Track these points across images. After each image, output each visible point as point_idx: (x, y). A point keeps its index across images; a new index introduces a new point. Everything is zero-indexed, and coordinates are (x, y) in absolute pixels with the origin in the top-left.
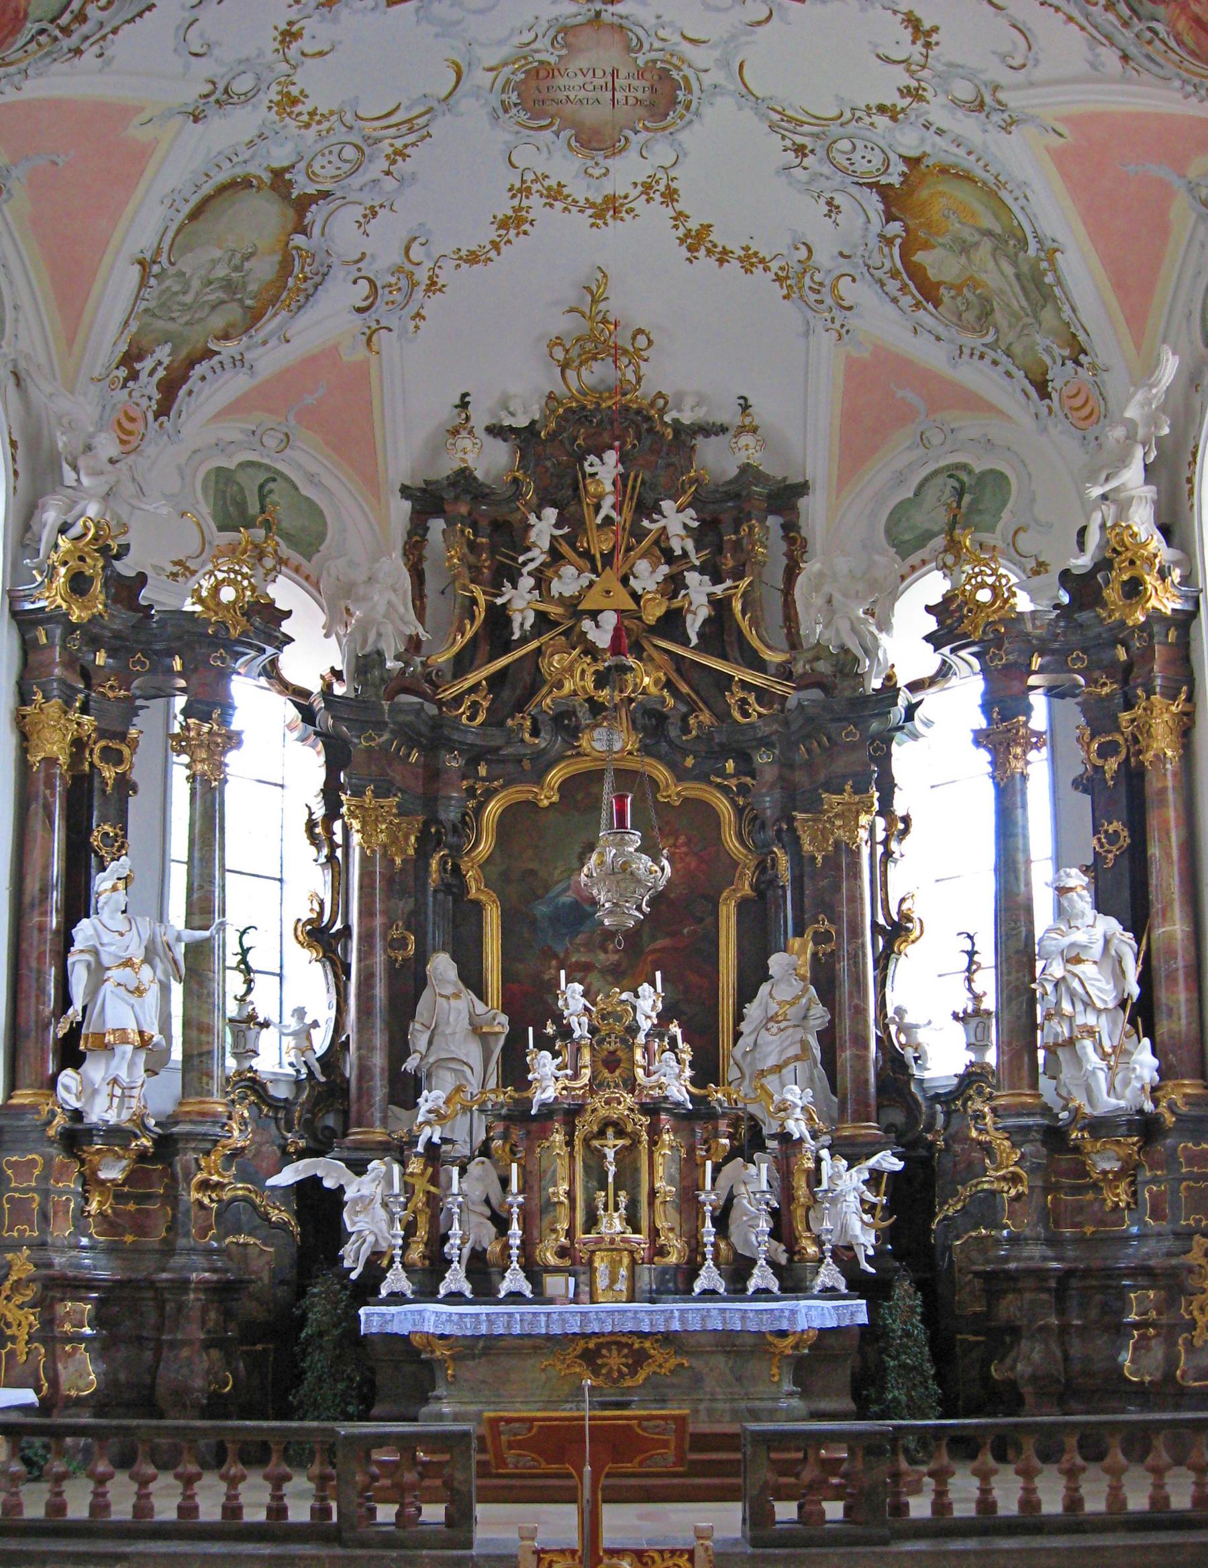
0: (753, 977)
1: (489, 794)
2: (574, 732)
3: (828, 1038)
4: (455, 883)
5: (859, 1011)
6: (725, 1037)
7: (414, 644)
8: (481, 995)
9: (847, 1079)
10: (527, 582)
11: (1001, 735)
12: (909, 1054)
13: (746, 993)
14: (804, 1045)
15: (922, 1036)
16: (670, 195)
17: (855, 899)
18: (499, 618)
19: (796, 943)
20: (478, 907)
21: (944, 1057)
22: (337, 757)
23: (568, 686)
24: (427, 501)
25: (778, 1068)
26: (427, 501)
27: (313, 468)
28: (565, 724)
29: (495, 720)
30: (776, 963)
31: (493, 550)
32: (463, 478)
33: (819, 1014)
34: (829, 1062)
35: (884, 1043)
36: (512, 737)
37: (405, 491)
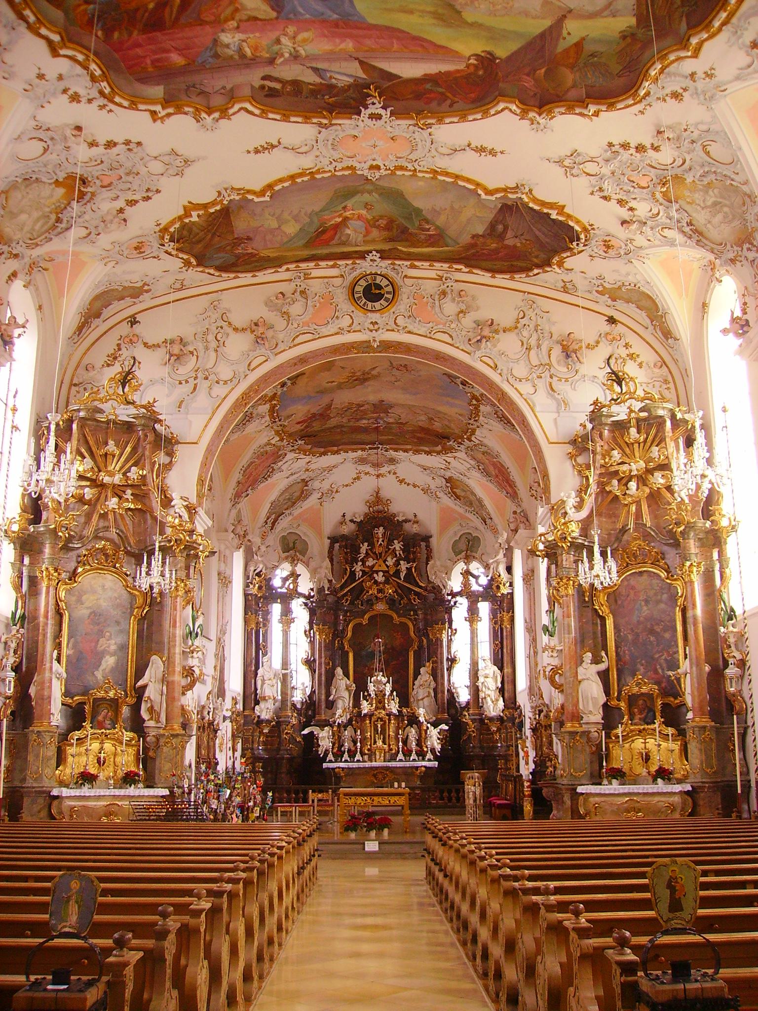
0: (417, 674)
1: (350, 621)
2: (372, 605)
3: (435, 690)
4: (342, 647)
5: (443, 684)
6: (410, 690)
7: (330, 581)
8: (348, 676)
9: (440, 701)
10: (360, 563)
11: (473, 615)
12: (455, 695)
13: (415, 678)
14: (429, 693)
15: (459, 690)
16: (395, 473)
17: (442, 653)
18: (353, 573)
19: (428, 664)
20: (347, 653)
21: (464, 696)
22: (312, 613)
23: (370, 592)
24: (333, 540)
25: (422, 699)
26: (333, 540)
27: (305, 531)
28: (370, 603)
29: (352, 603)
30: (422, 670)
31: (351, 552)
32: (344, 537)
33: (433, 683)
34: (435, 696)
35: (448, 690)
36: (356, 606)
37: (329, 538)
